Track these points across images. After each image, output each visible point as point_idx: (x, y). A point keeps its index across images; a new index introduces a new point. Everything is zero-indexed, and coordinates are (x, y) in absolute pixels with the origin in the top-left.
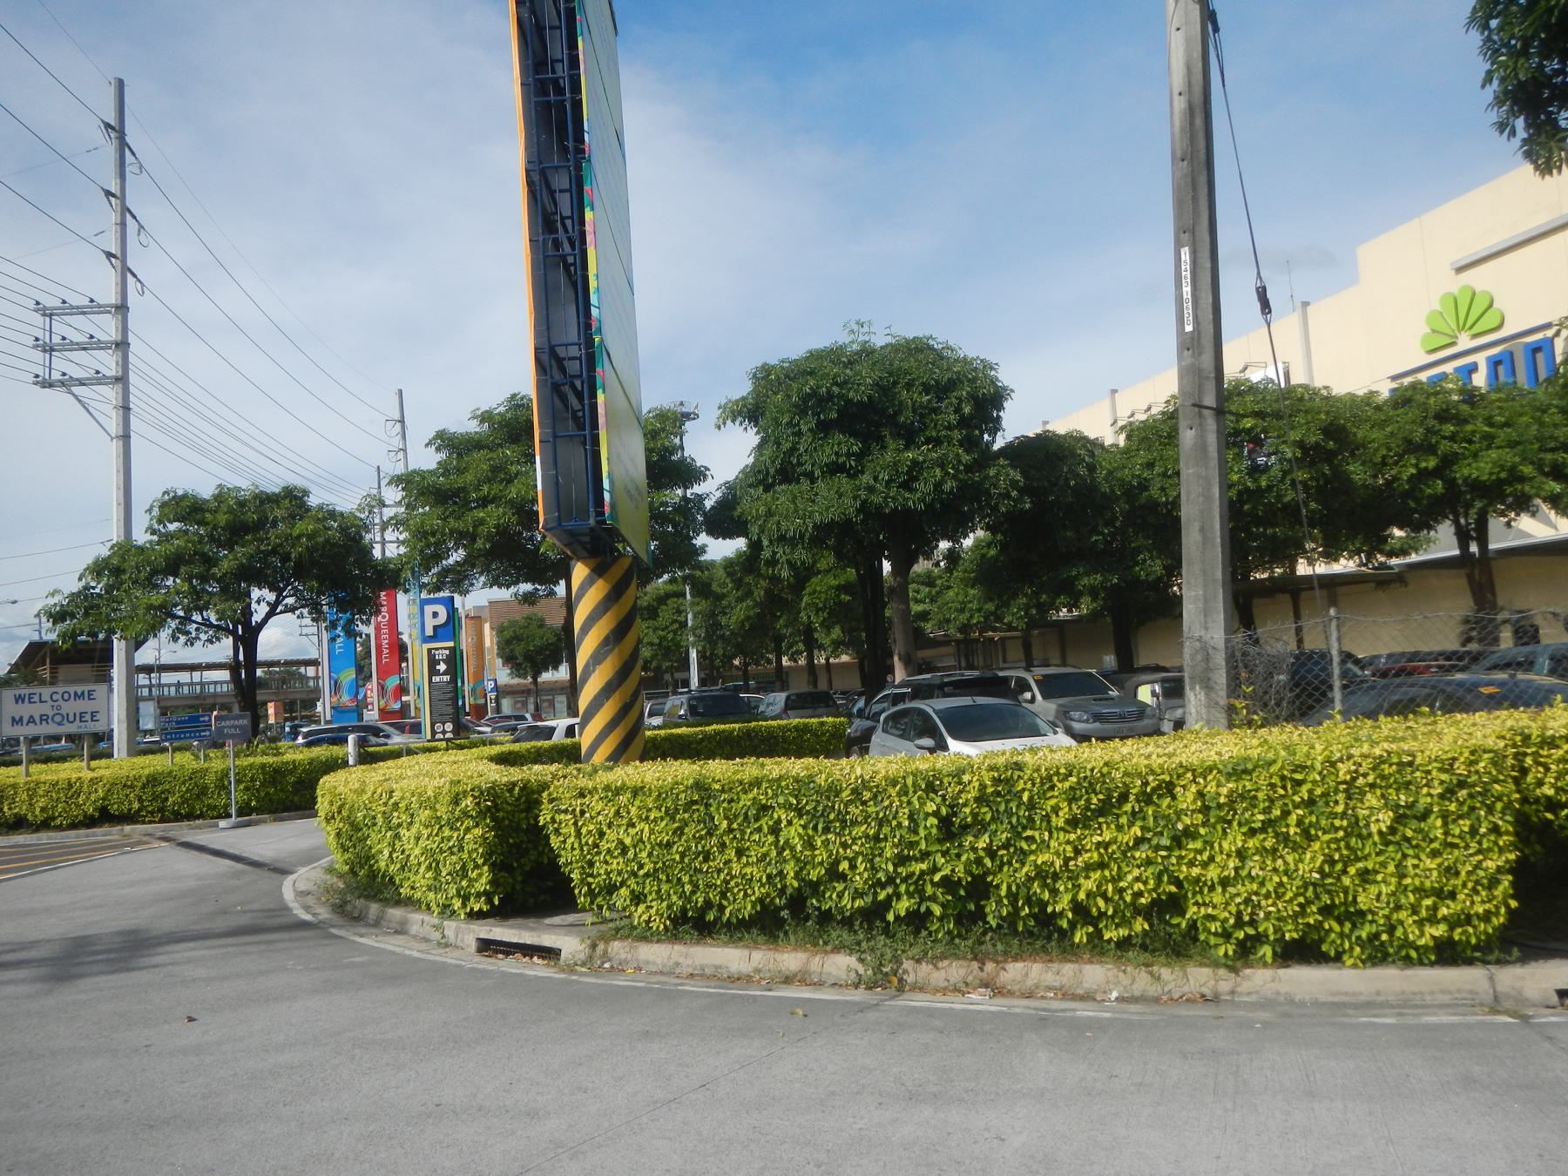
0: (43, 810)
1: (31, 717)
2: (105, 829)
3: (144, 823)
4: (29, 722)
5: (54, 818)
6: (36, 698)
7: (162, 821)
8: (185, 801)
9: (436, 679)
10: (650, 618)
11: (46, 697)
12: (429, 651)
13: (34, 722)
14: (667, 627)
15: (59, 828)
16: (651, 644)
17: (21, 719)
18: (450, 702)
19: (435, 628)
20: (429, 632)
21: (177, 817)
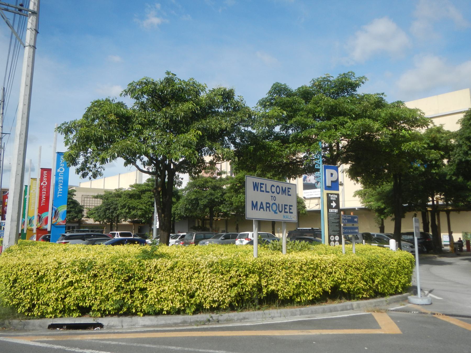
0: (299, 286)
1: (262, 203)
2: (336, 304)
3: (358, 298)
4: (260, 208)
5: (298, 295)
6: (263, 189)
7: (371, 297)
8: (384, 282)
9: (331, 211)
10: (137, 199)
11: (268, 189)
12: (328, 194)
13: (263, 208)
14: (146, 203)
15: (300, 303)
16: (141, 209)
17: (257, 202)
18: (338, 224)
19: (332, 182)
20: (329, 184)
21: (377, 294)
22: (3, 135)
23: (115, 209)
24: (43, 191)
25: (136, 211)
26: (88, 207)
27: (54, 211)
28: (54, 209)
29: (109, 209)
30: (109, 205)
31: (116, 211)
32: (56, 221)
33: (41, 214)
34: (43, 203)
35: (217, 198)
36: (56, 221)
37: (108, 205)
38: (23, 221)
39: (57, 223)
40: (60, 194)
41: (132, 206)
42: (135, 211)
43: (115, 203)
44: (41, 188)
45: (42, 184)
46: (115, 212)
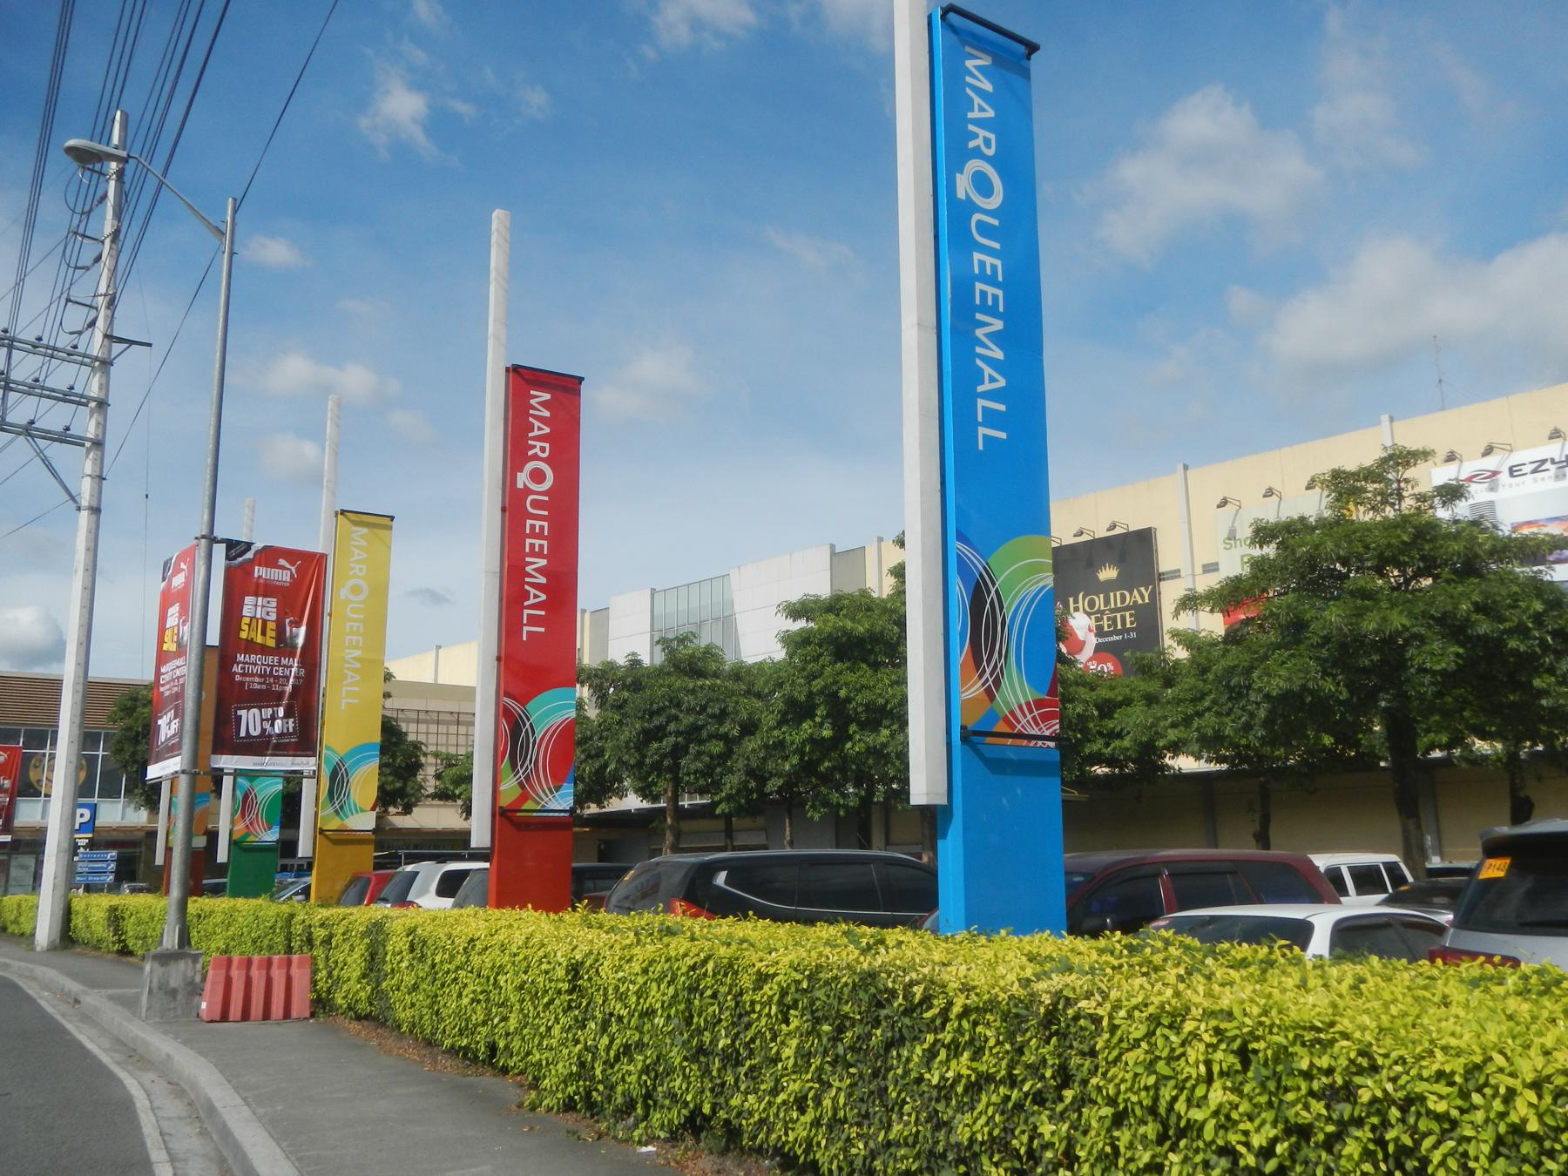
22: (117, 348)
23: (693, 734)
24: (533, 535)
25: (892, 735)
26: (443, 749)
27: (958, 587)
28: (962, 563)
29: (657, 734)
30: (659, 712)
31: (701, 742)
32: (990, 694)
33: (524, 704)
34: (533, 620)
35: (1521, 631)
36: (990, 694)
37: (652, 714)
38: (240, 795)
39: (993, 716)
40: (992, 419)
41: (868, 707)
42: (886, 732)
43: (688, 700)
44: (514, 507)
45: (522, 479)
46: (693, 748)
